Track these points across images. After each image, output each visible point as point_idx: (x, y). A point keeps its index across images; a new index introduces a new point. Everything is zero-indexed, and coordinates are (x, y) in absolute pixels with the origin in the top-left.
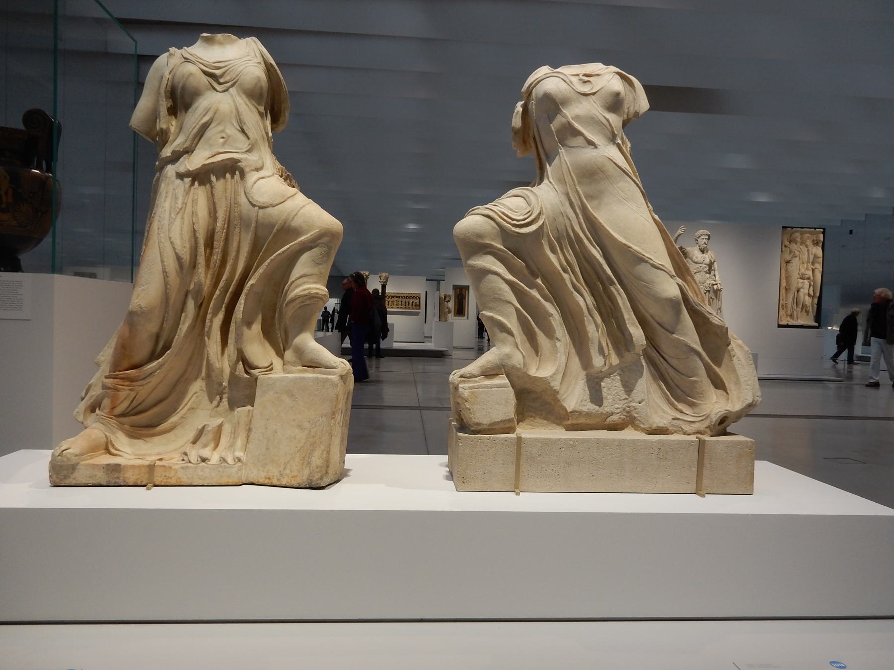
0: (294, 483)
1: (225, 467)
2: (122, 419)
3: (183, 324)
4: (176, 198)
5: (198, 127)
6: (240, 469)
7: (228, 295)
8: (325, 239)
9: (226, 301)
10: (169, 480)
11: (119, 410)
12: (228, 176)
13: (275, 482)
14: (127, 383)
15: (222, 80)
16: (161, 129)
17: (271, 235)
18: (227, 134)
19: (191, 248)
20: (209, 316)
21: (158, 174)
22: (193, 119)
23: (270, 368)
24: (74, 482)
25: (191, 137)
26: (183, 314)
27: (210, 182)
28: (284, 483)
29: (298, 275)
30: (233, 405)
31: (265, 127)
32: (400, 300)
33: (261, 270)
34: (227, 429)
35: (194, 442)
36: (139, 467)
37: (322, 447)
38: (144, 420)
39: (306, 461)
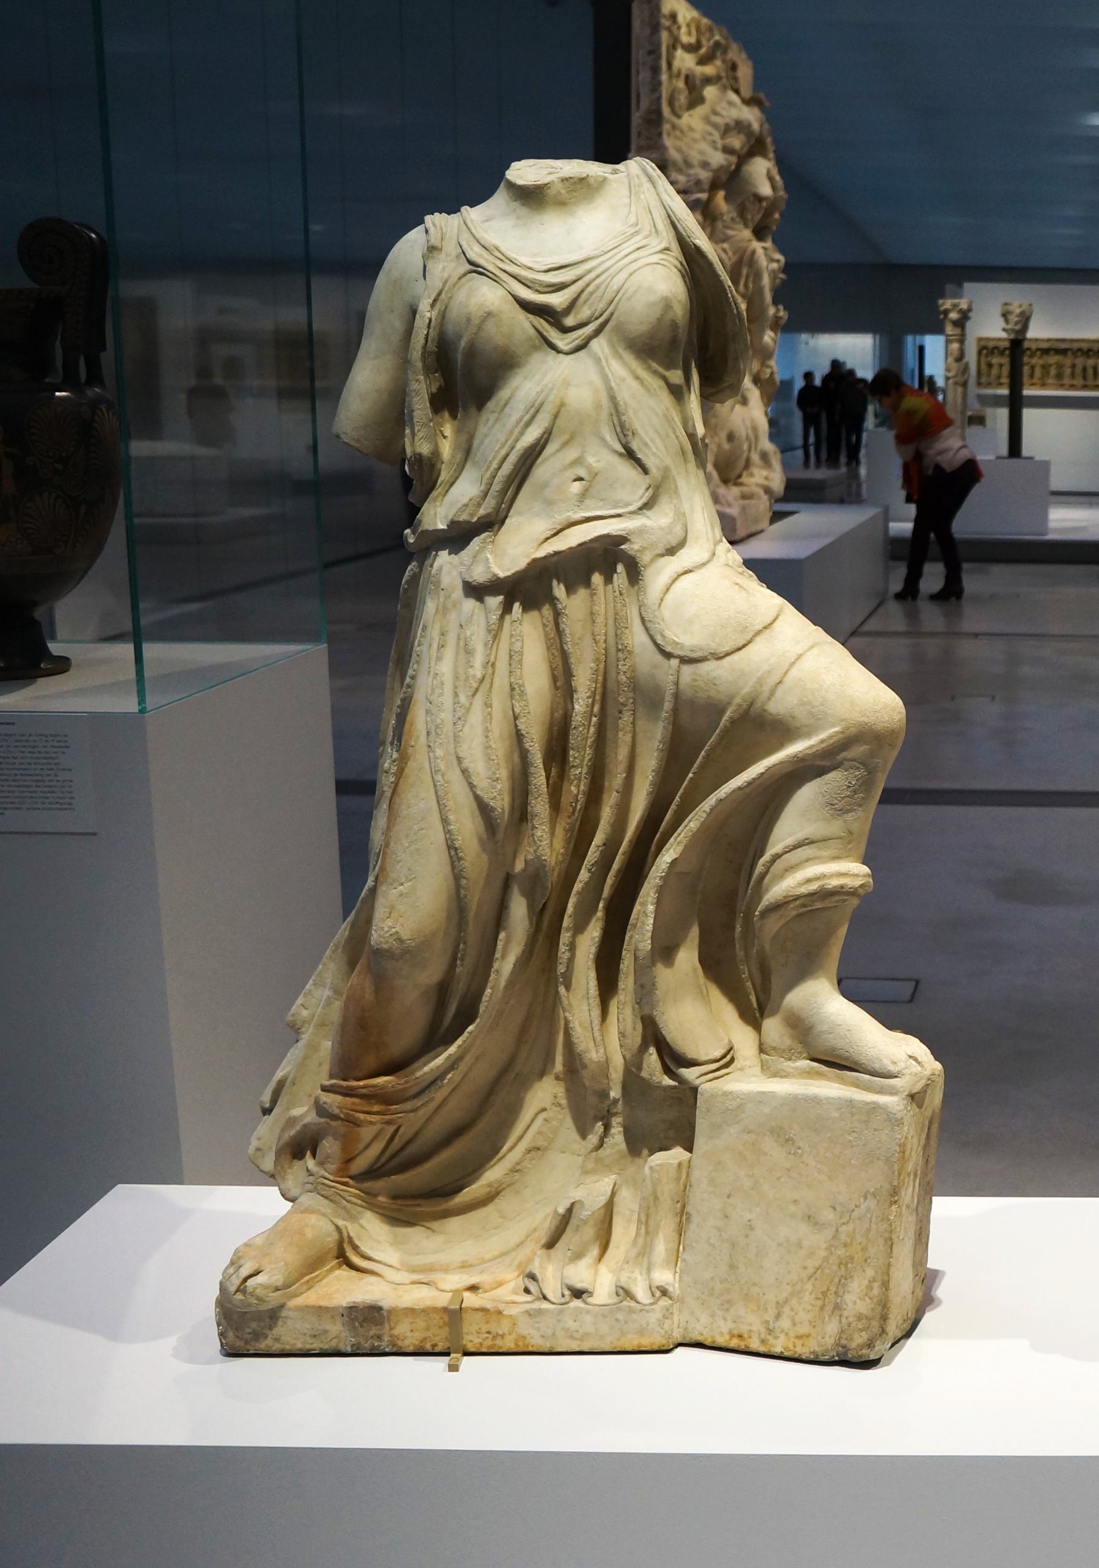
0: (803, 1351)
1: (631, 1311)
2: (368, 1185)
3: (503, 957)
4: (469, 652)
5: (513, 458)
6: (668, 1314)
7: (610, 880)
8: (859, 751)
9: (606, 892)
10: (499, 1342)
11: (361, 1164)
12: (597, 579)
13: (755, 1346)
14: (376, 1108)
15: (569, 321)
16: (419, 458)
17: (714, 732)
18: (589, 468)
19: (512, 777)
20: (565, 937)
21: (412, 567)
22: (503, 429)
23: (727, 1060)
24: (276, 1347)
25: (496, 487)
26: (502, 935)
27: (552, 600)
28: (778, 1350)
29: (790, 841)
30: (640, 1143)
31: (686, 421)
32: (1068, 361)
33: (692, 823)
34: (628, 1203)
35: (550, 1245)
36: (426, 1312)
37: (870, 1272)
38: (422, 1175)
39: (830, 1302)
